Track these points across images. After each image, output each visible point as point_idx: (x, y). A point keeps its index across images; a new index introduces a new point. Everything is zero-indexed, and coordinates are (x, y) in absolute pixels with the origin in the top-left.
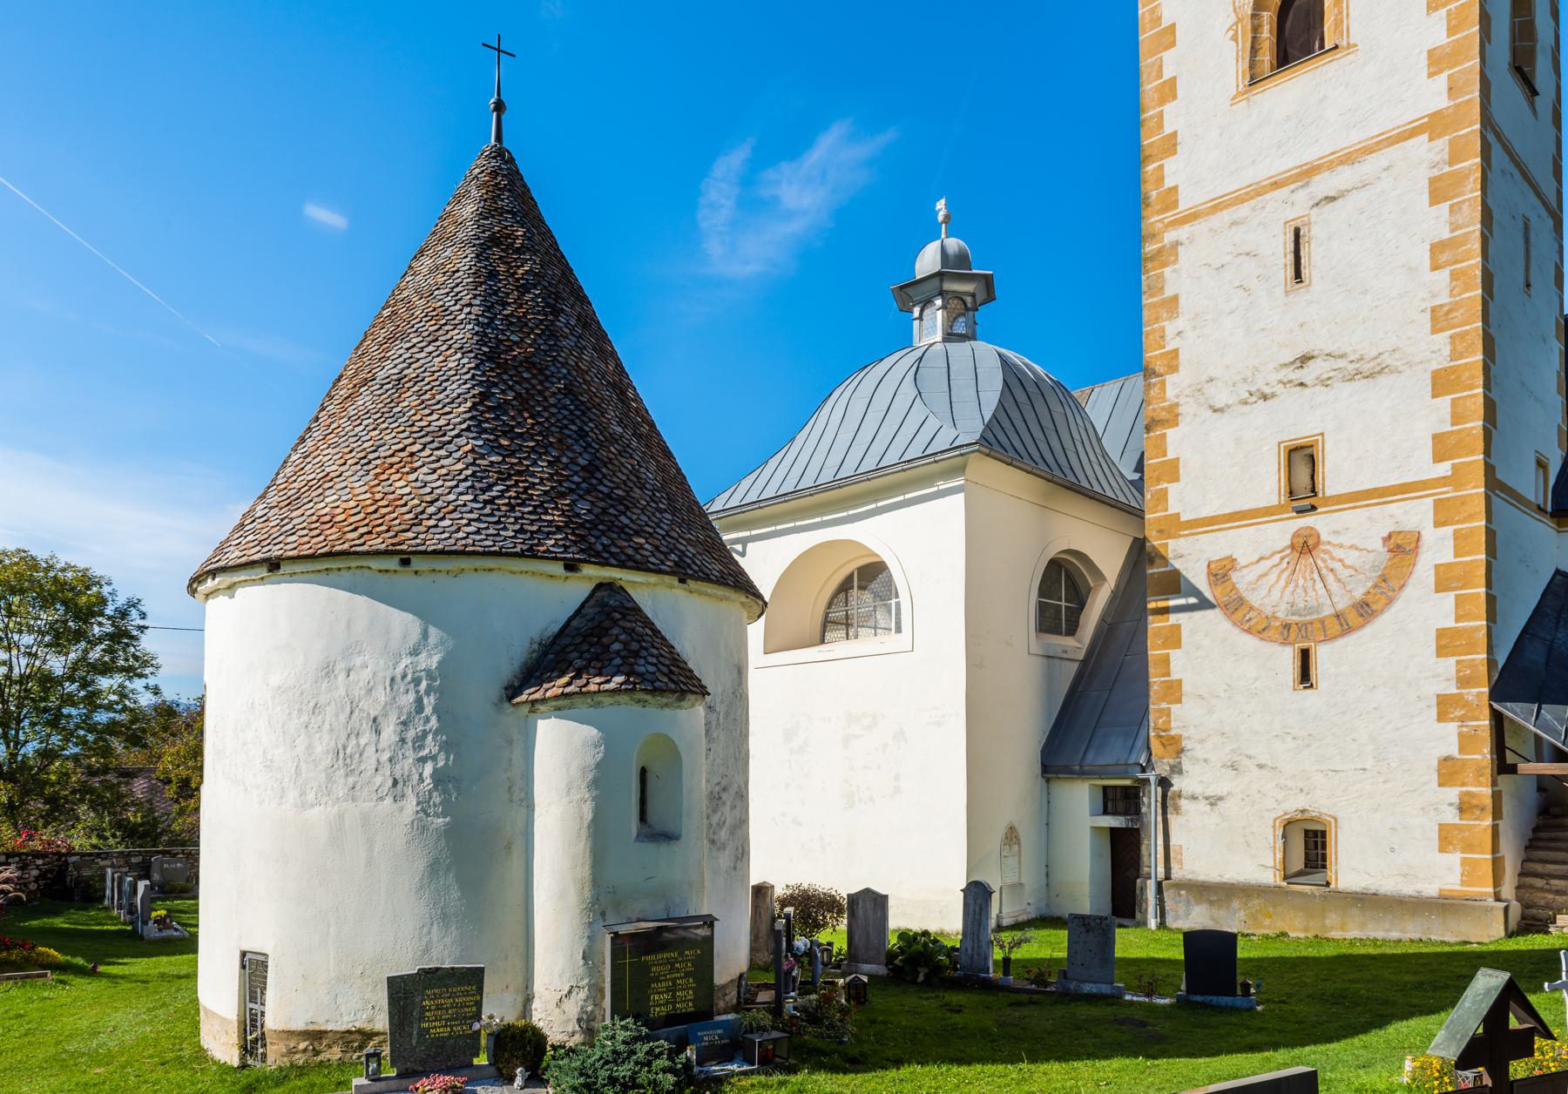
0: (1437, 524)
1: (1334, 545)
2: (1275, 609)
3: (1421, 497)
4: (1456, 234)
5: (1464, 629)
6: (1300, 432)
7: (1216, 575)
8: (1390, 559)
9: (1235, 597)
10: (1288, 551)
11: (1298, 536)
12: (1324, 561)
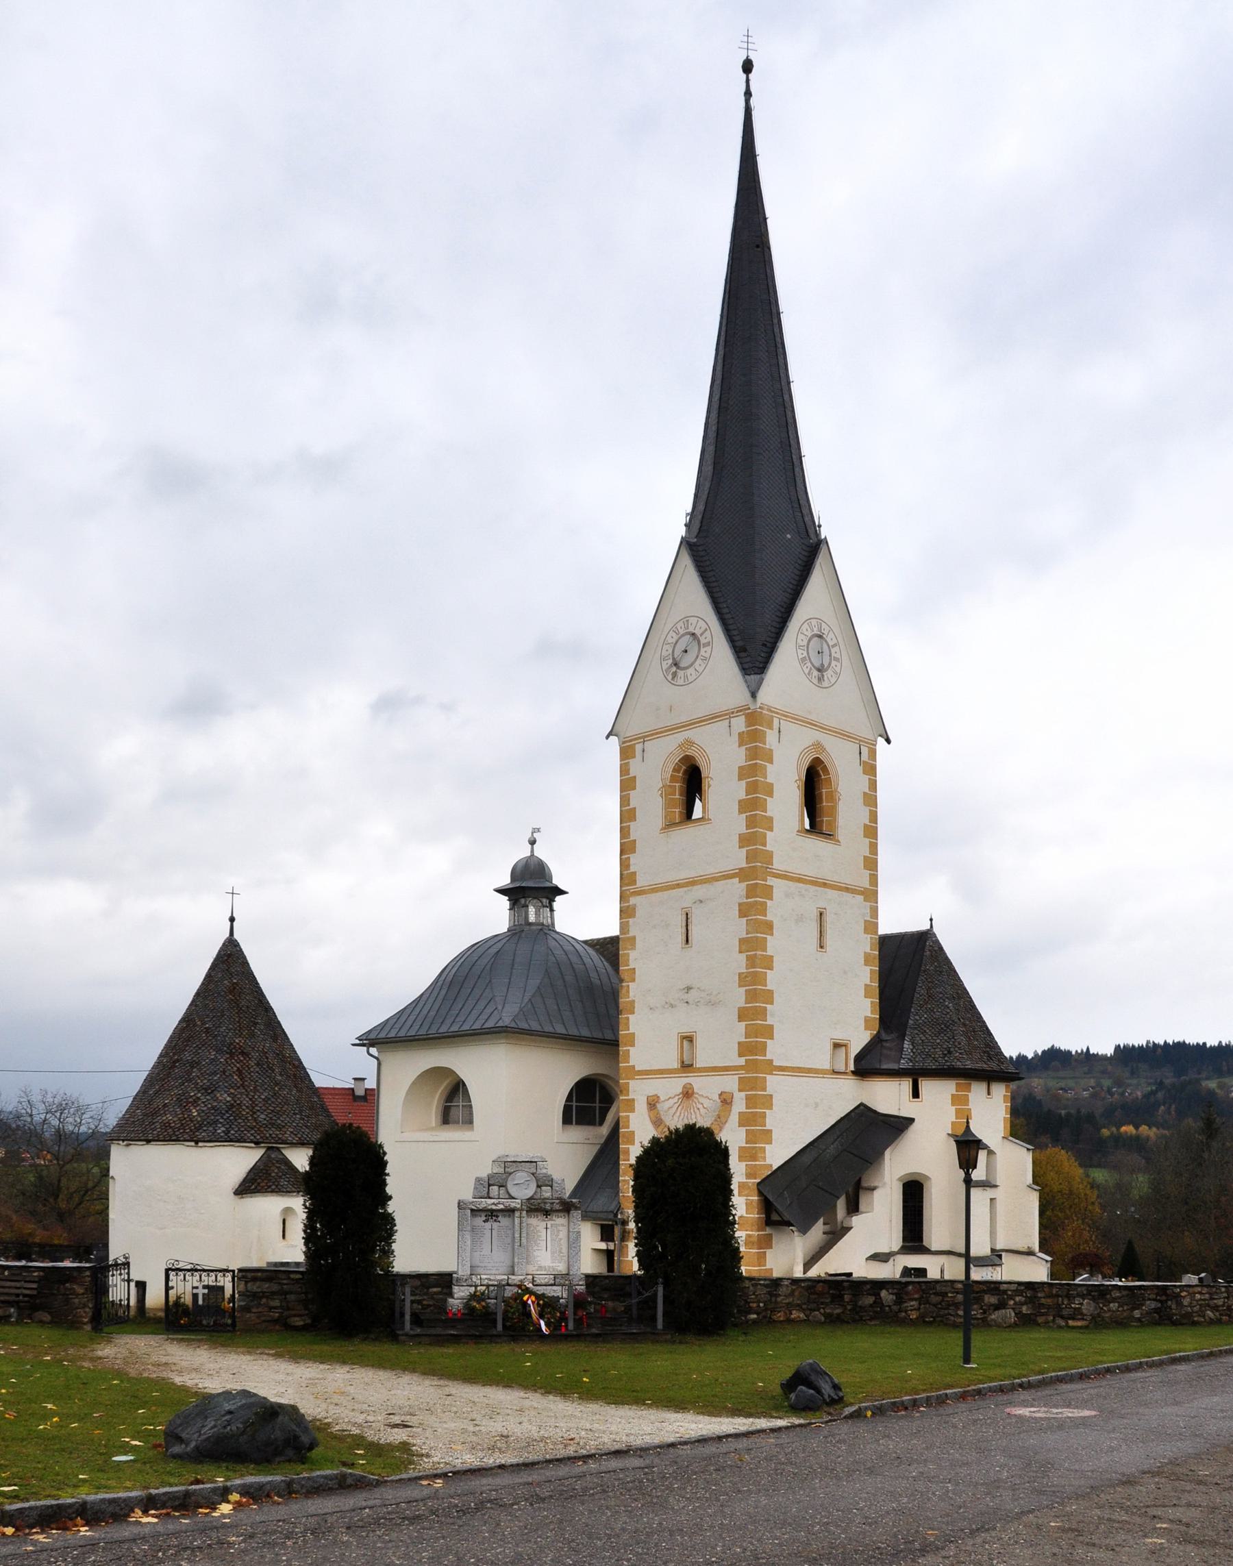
0: (740, 1090)
1: (700, 1095)
4: (749, 935)
6: (686, 1030)
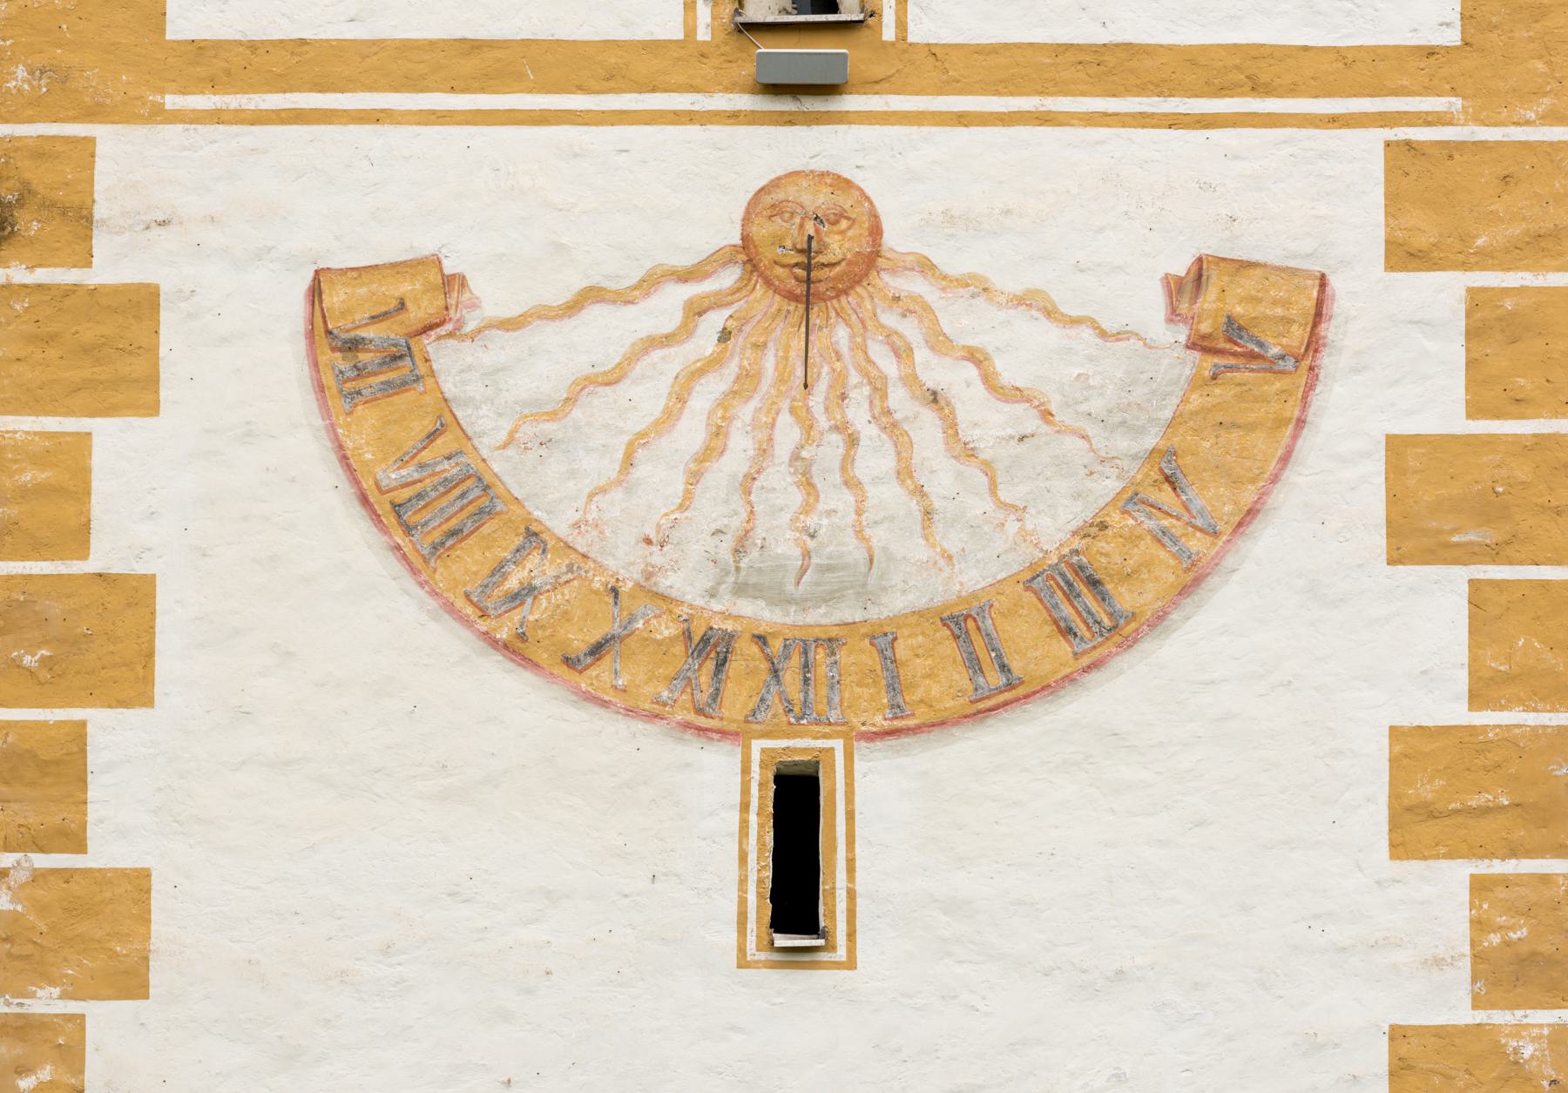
1: (949, 282)
2: (657, 558)
3: (1334, 121)
5: (1509, 738)
7: (353, 346)
8: (1196, 383)
9: (450, 469)
10: (728, 278)
11: (776, 210)
12: (902, 352)
